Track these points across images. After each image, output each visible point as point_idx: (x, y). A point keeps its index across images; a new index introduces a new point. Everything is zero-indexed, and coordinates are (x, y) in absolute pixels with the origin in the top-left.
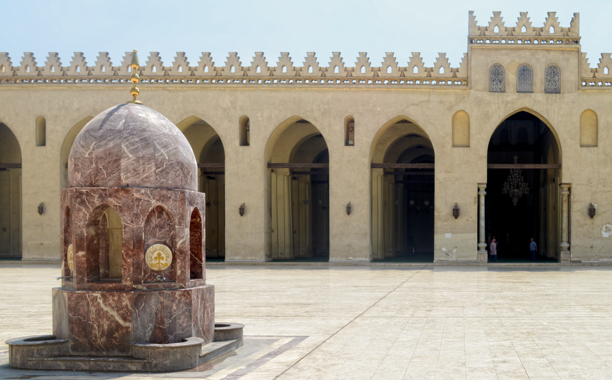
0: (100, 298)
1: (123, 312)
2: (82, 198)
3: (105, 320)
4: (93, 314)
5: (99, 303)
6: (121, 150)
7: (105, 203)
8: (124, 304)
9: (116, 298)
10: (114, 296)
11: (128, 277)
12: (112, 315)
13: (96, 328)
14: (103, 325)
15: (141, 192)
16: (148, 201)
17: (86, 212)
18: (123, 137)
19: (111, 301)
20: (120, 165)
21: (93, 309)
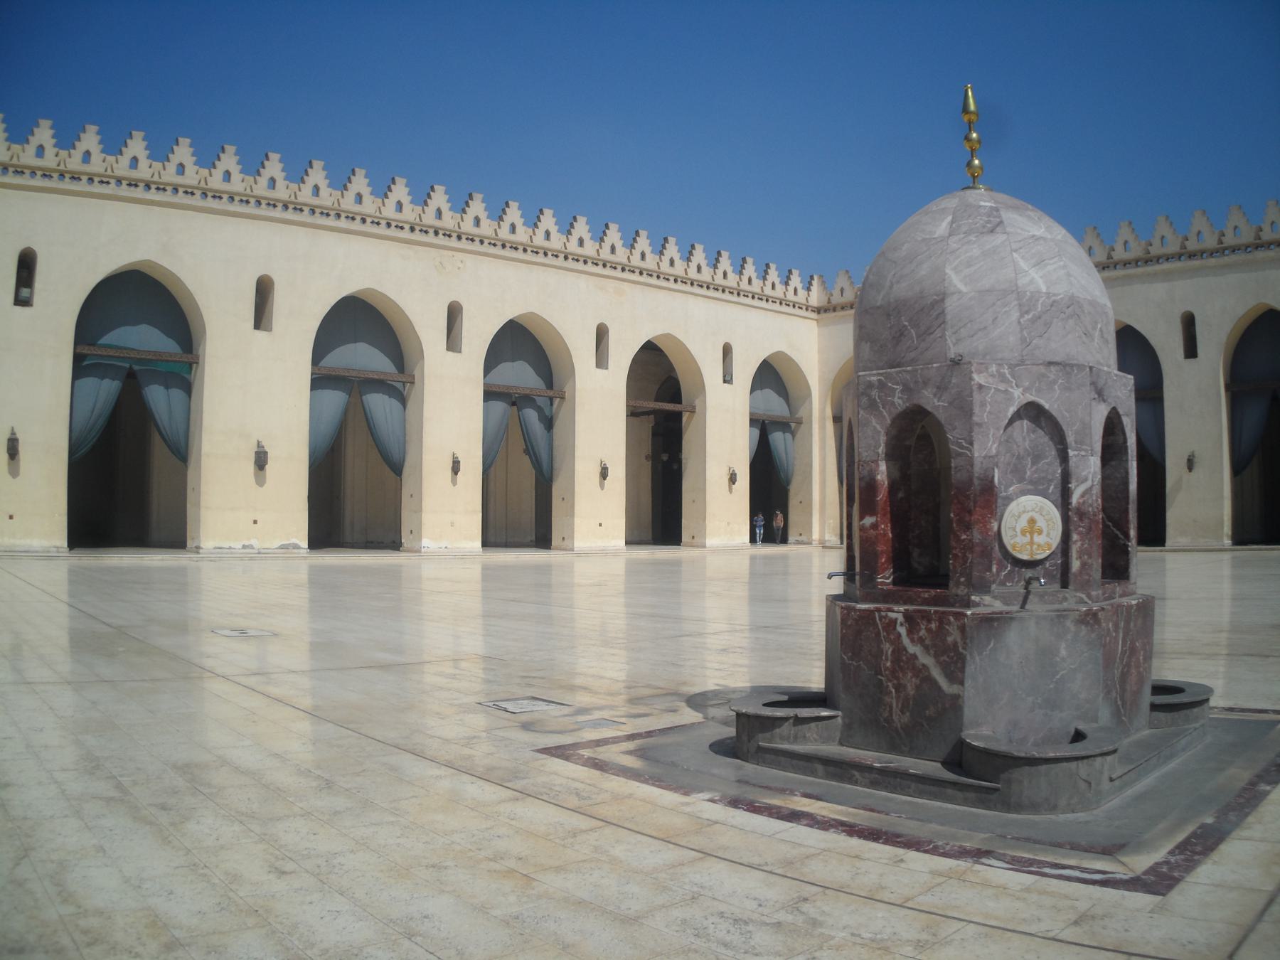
0: (902, 625)
1: (947, 659)
2: (869, 396)
3: (910, 675)
4: (887, 660)
5: (899, 635)
6: (944, 280)
7: (915, 402)
8: (950, 639)
9: (933, 626)
10: (929, 621)
11: (962, 575)
12: (924, 665)
13: (891, 692)
14: (905, 687)
15: (990, 370)
16: (1006, 390)
17: (878, 427)
18: (948, 251)
19: (923, 633)
20: (943, 312)
21: (888, 648)
